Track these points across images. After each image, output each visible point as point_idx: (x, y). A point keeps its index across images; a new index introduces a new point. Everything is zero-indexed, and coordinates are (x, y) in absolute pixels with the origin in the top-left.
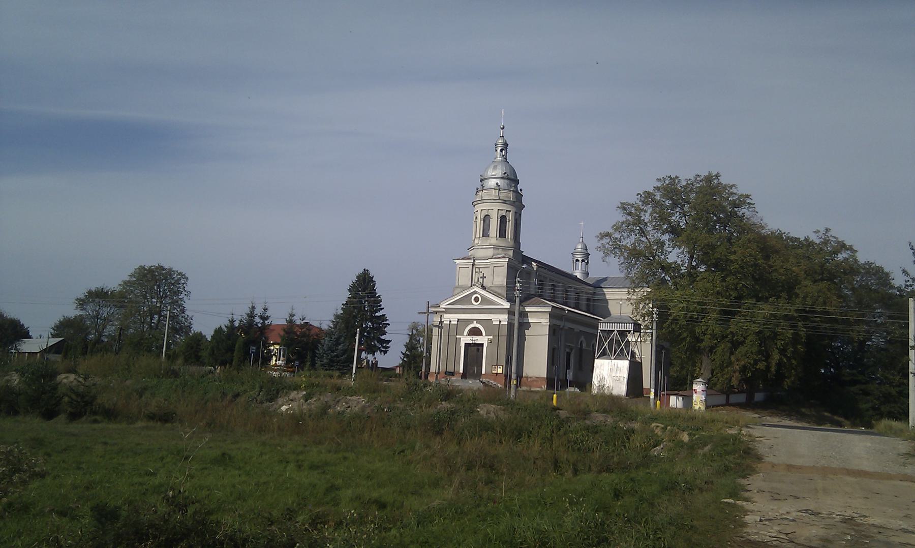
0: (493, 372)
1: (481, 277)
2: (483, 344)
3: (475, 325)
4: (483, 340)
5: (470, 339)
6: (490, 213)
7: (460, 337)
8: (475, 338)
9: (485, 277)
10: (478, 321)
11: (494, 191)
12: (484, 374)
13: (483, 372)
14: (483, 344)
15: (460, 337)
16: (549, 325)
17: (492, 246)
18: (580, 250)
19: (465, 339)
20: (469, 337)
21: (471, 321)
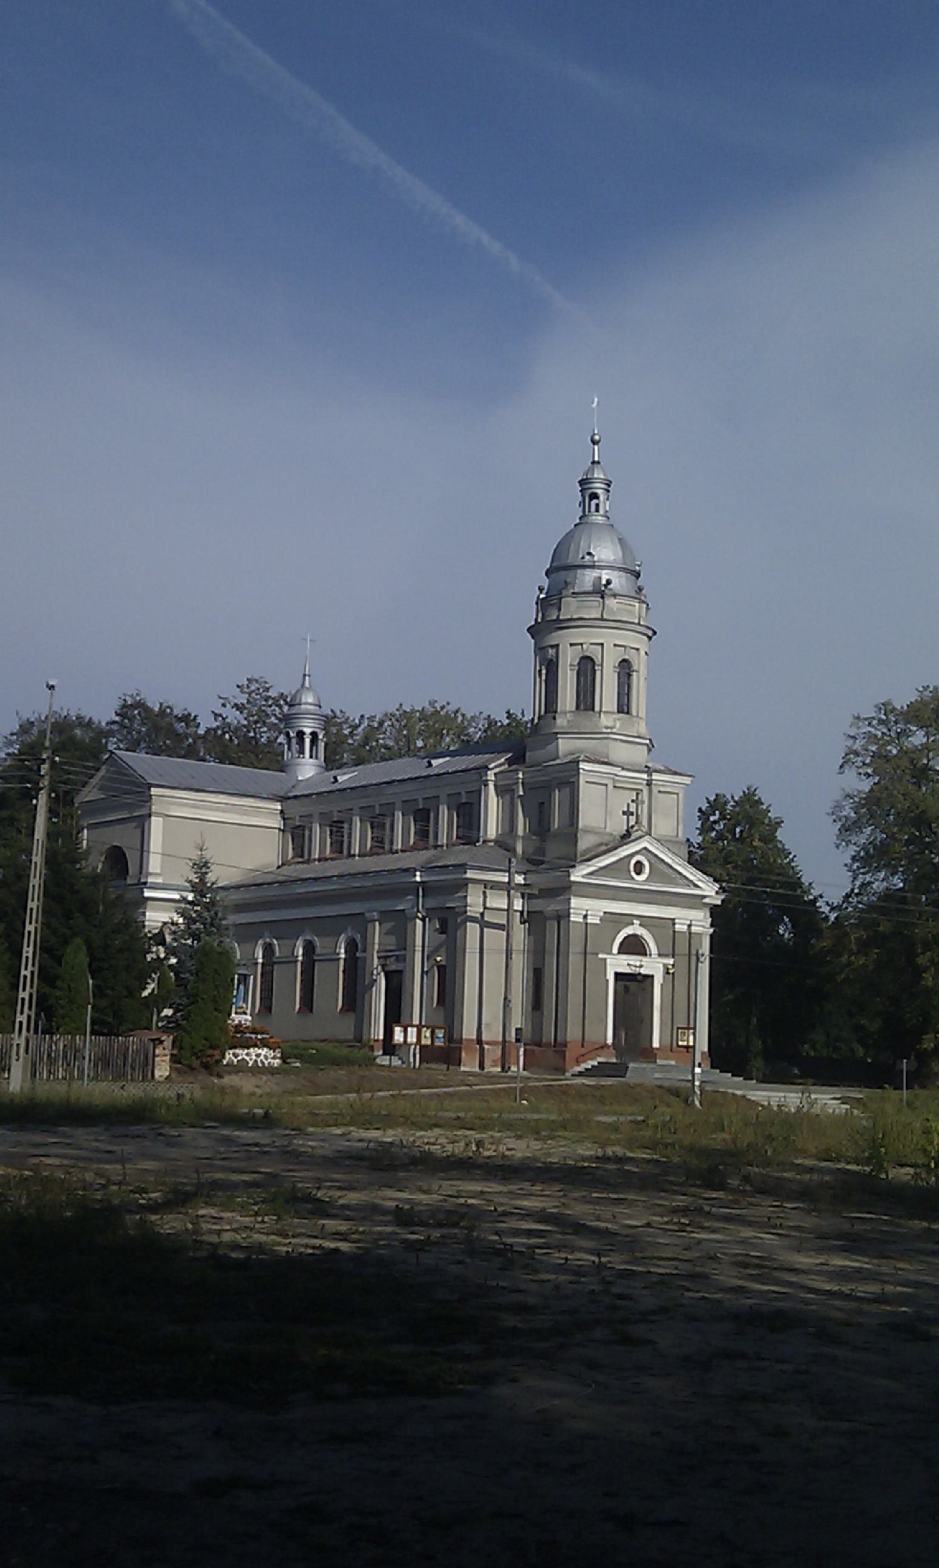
0: (680, 1043)
1: (632, 814)
2: (652, 976)
3: (635, 929)
4: (653, 966)
5: (626, 962)
6: (631, 656)
7: (604, 956)
8: (645, 960)
9: (624, 813)
10: (645, 921)
11: (637, 605)
12: (657, 1049)
13: (656, 1044)
14: (652, 976)
15: (604, 956)
16: (711, 936)
17: (648, 742)
18: (312, 707)
19: (618, 963)
20: (624, 957)
21: (627, 919)
